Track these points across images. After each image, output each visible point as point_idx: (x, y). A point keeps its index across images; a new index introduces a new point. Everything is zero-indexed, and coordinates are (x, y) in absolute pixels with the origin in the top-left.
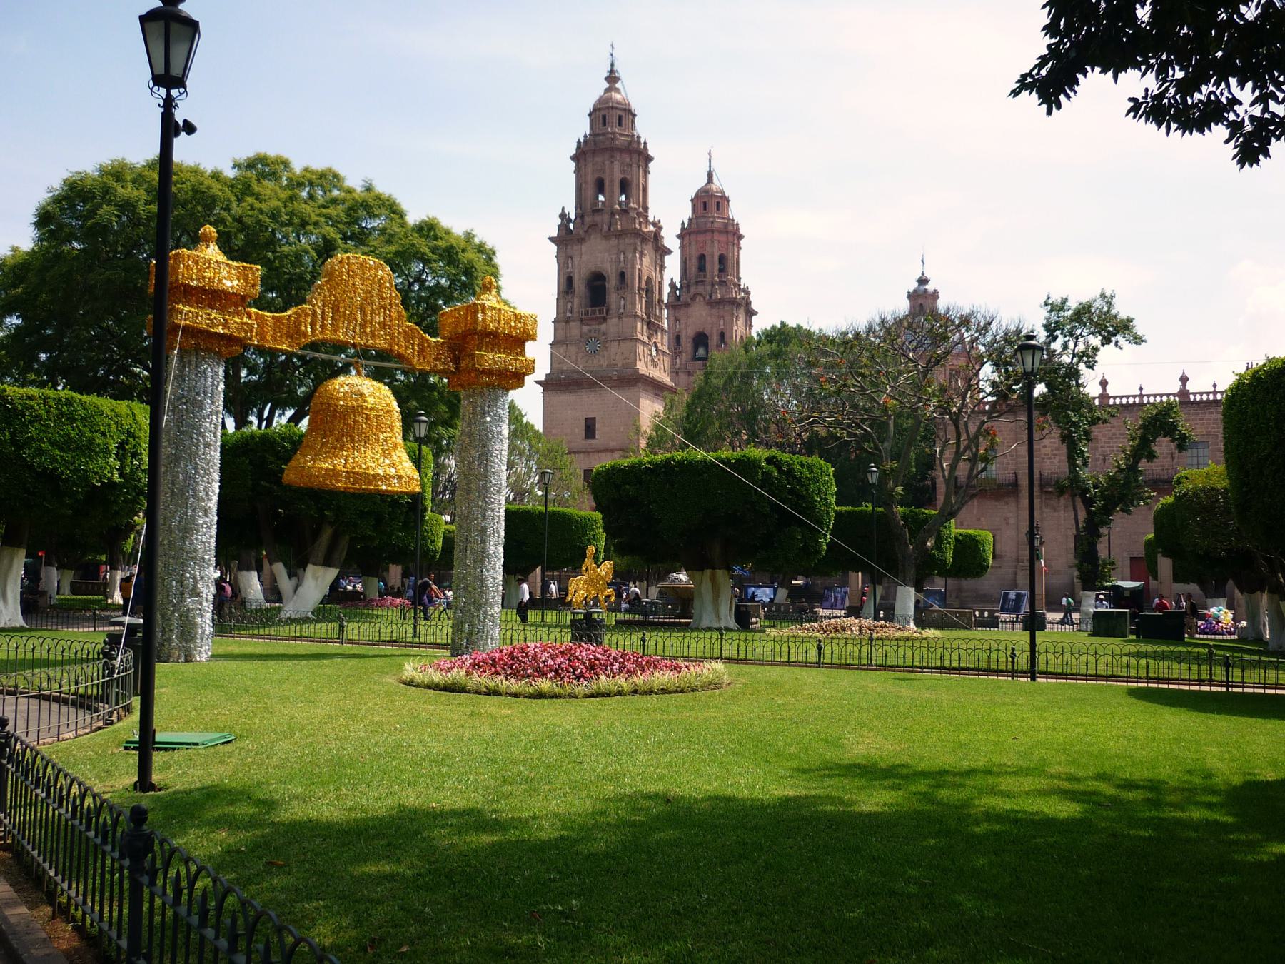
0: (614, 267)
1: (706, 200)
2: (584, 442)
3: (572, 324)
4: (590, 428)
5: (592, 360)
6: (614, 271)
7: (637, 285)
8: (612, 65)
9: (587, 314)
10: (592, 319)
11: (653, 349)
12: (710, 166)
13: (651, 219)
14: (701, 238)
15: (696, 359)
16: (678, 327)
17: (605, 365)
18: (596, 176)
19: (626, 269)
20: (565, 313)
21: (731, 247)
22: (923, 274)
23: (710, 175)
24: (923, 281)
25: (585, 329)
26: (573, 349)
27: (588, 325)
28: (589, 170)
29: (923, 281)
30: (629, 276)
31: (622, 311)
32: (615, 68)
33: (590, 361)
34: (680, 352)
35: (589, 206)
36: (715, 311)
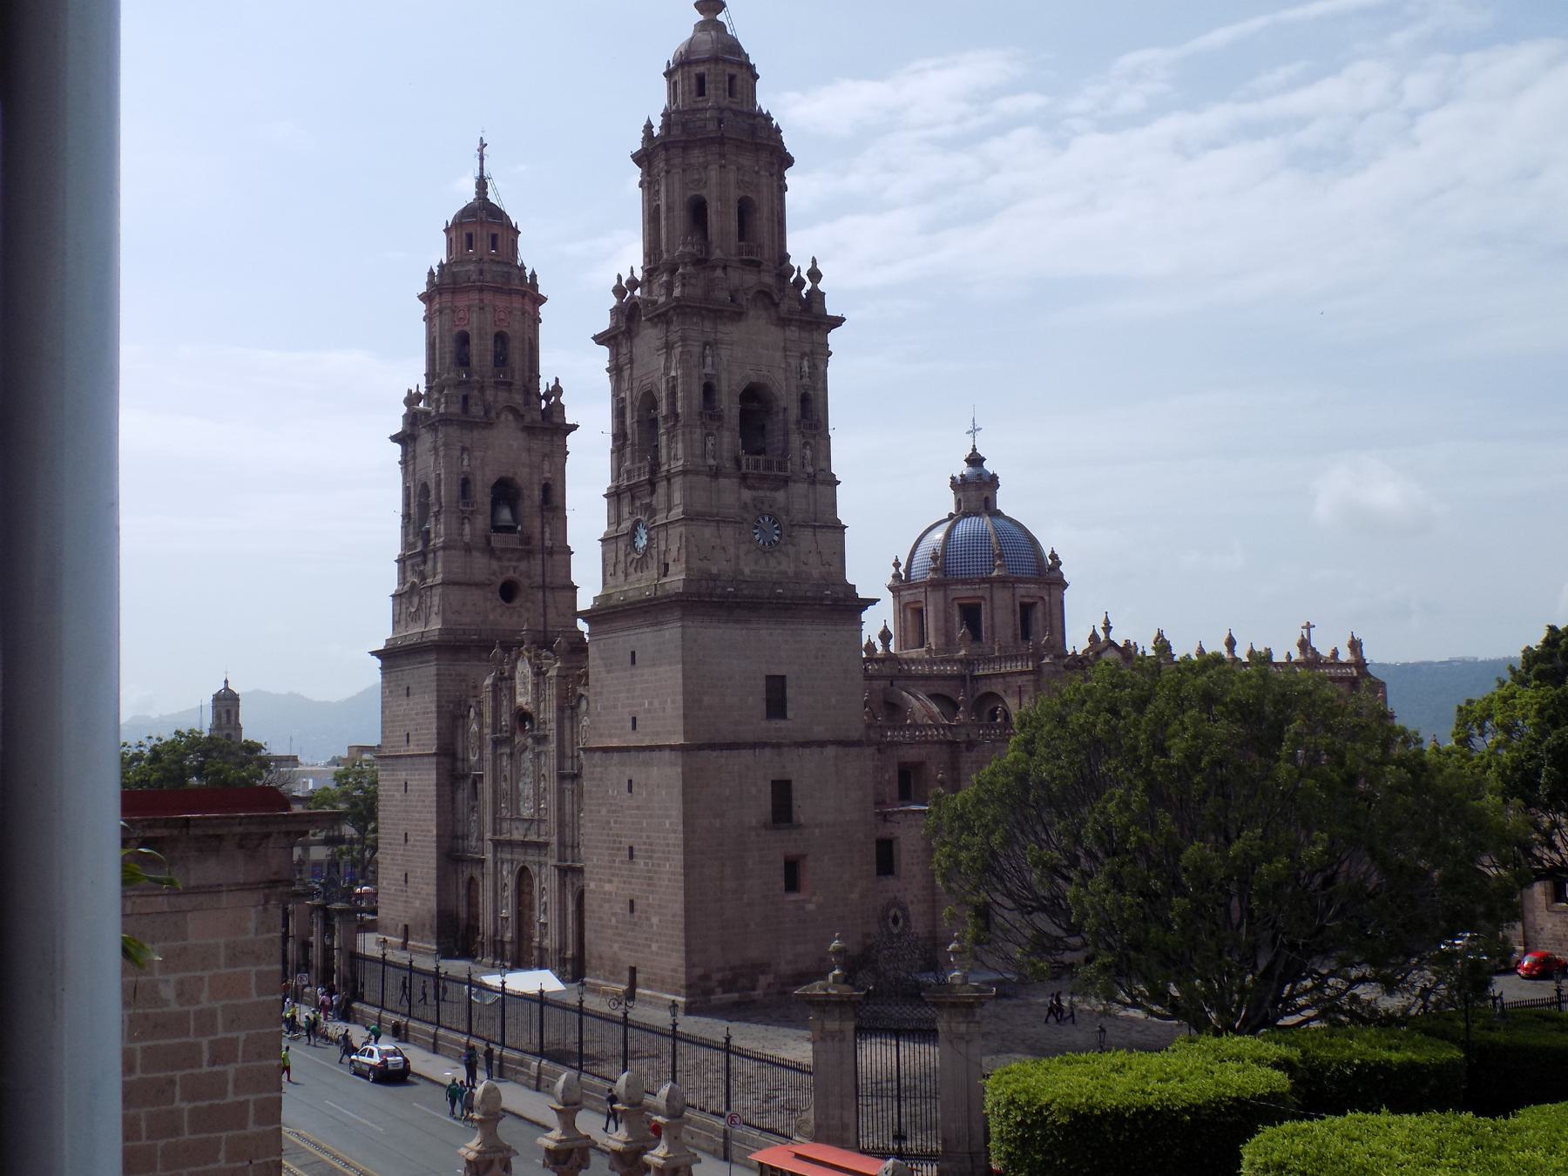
1: (496, 230)
2: (764, 724)
3: (723, 482)
4: (776, 697)
9: (756, 467)
10: (763, 478)
12: (482, 169)
14: (501, 302)
15: (497, 529)
16: (466, 462)
18: (742, 194)
22: (974, 449)
23: (482, 184)
24: (975, 460)
25: (747, 495)
26: (728, 532)
27: (749, 488)
28: (732, 177)
29: (975, 460)
33: (763, 562)
34: (472, 513)
35: (733, 252)
36: (536, 444)
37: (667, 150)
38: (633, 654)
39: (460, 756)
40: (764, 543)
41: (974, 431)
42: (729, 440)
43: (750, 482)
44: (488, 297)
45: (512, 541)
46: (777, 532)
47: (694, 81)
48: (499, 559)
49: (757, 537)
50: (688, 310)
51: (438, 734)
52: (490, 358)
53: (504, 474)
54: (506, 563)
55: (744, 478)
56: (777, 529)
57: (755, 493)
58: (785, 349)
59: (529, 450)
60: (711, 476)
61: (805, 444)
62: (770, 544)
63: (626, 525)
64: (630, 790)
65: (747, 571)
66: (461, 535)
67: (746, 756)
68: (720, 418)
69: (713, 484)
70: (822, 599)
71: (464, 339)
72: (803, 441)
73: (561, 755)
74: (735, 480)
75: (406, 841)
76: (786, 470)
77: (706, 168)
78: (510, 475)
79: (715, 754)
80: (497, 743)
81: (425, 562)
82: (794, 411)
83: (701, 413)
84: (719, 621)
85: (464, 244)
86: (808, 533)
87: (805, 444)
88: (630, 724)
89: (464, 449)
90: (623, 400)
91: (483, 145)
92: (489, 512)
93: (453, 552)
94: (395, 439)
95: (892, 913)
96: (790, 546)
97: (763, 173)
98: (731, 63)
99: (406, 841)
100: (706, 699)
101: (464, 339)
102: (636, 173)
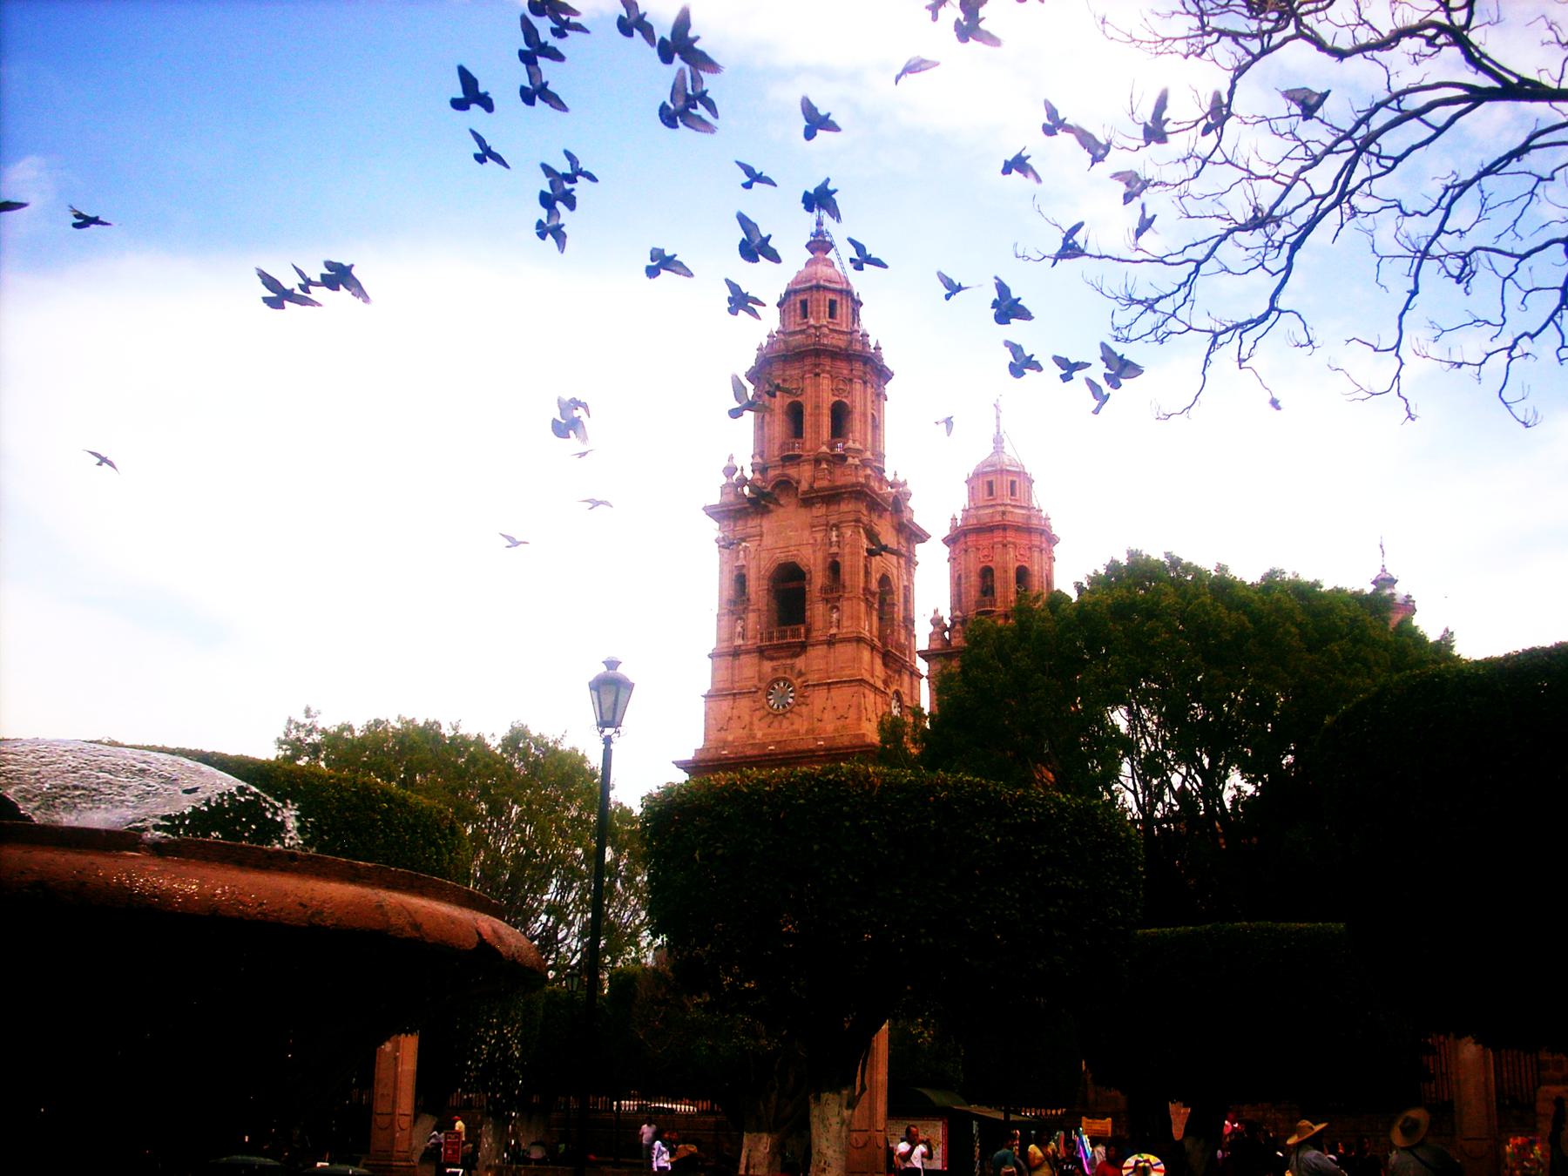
0: (820, 555)
1: (989, 479)
5: (781, 723)
6: (820, 561)
7: (862, 585)
11: (894, 703)
12: (998, 426)
13: (889, 476)
17: (802, 731)
20: (731, 639)
21: (1036, 554)
22: (1384, 570)
23: (998, 441)
25: (768, 666)
27: (772, 659)
31: (834, 631)
33: (776, 724)
40: (778, 707)
43: (766, 653)
46: (792, 695)
49: (772, 702)
56: (791, 692)
57: (775, 663)
62: (784, 707)
65: (759, 734)
69: (737, 662)
74: (755, 654)
86: (823, 692)
96: (804, 706)
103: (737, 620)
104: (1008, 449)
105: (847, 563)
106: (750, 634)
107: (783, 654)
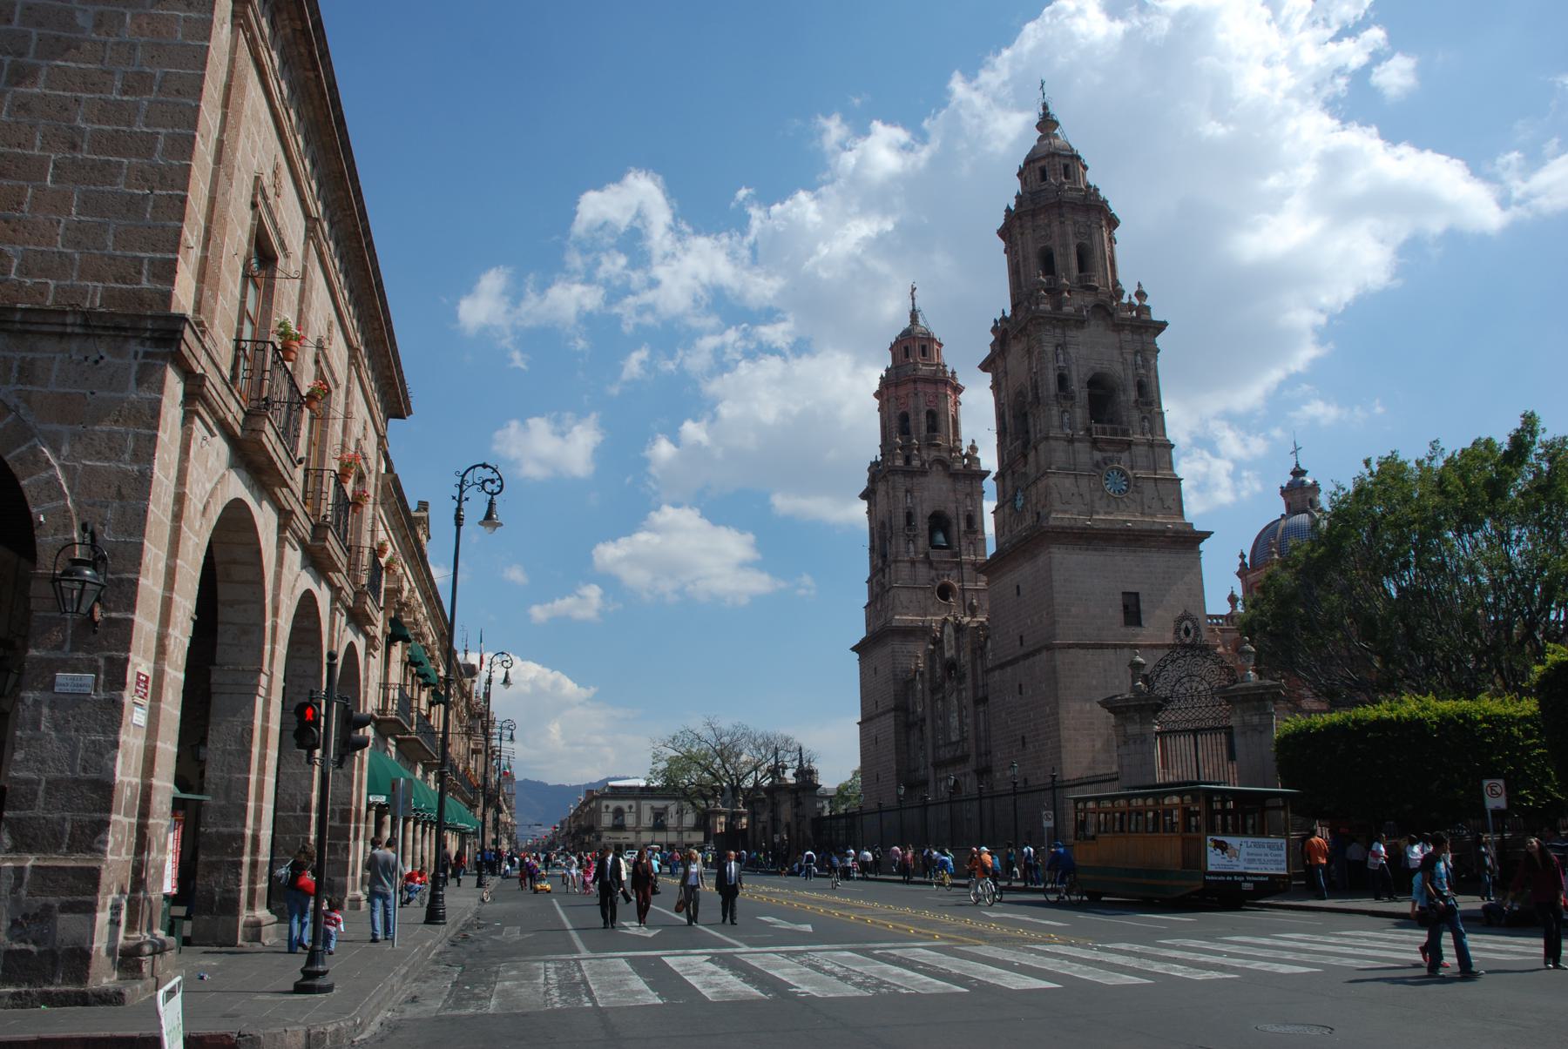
2: (1123, 630)
3: (1077, 445)
6: (1131, 376)
8: (1045, 107)
12: (913, 305)
14: (930, 389)
15: (934, 547)
16: (909, 500)
18: (1079, 241)
19: (1147, 377)
22: (1297, 465)
24: (1298, 472)
25: (1098, 456)
26: (1083, 482)
27: (1100, 450)
29: (1298, 472)
30: (1154, 388)
32: (1051, 109)
34: (915, 536)
37: (1020, 219)
38: (1018, 587)
39: (911, 710)
41: (1296, 451)
42: (1080, 414)
44: (920, 386)
45: (944, 555)
47: (1038, 172)
48: (936, 569)
50: (1041, 320)
51: (895, 695)
52: (924, 428)
53: (937, 509)
54: (942, 572)
55: (1095, 443)
57: (1105, 455)
58: (1121, 348)
59: (955, 491)
60: (1069, 441)
61: (1144, 418)
63: (1010, 492)
64: (1021, 693)
66: (908, 552)
67: (1109, 653)
68: (1072, 398)
70: (1164, 532)
71: (904, 418)
72: (1141, 415)
73: (975, 687)
75: (878, 779)
76: (1128, 435)
77: (1049, 226)
78: (942, 509)
79: (1082, 652)
80: (933, 691)
81: (884, 577)
82: (1133, 394)
83: (1056, 395)
84: (1080, 549)
85: (903, 354)
87: (1144, 418)
88: (1018, 643)
89: (907, 491)
90: (1003, 404)
91: (914, 289)
92: (927, 536)
93: (901, 564)
94: (864, 496)
95: (1183, 626)
97: (1093, 225)
98: (1065, 156)
99: (878, 779)
100: (1073, 609)
101: (904, 418)
102: (1001, 244)
103: (1063, 412)
104: (921, 322)
105: (1154, 384)
106: (1079, 426)
107: (1112, 448)
